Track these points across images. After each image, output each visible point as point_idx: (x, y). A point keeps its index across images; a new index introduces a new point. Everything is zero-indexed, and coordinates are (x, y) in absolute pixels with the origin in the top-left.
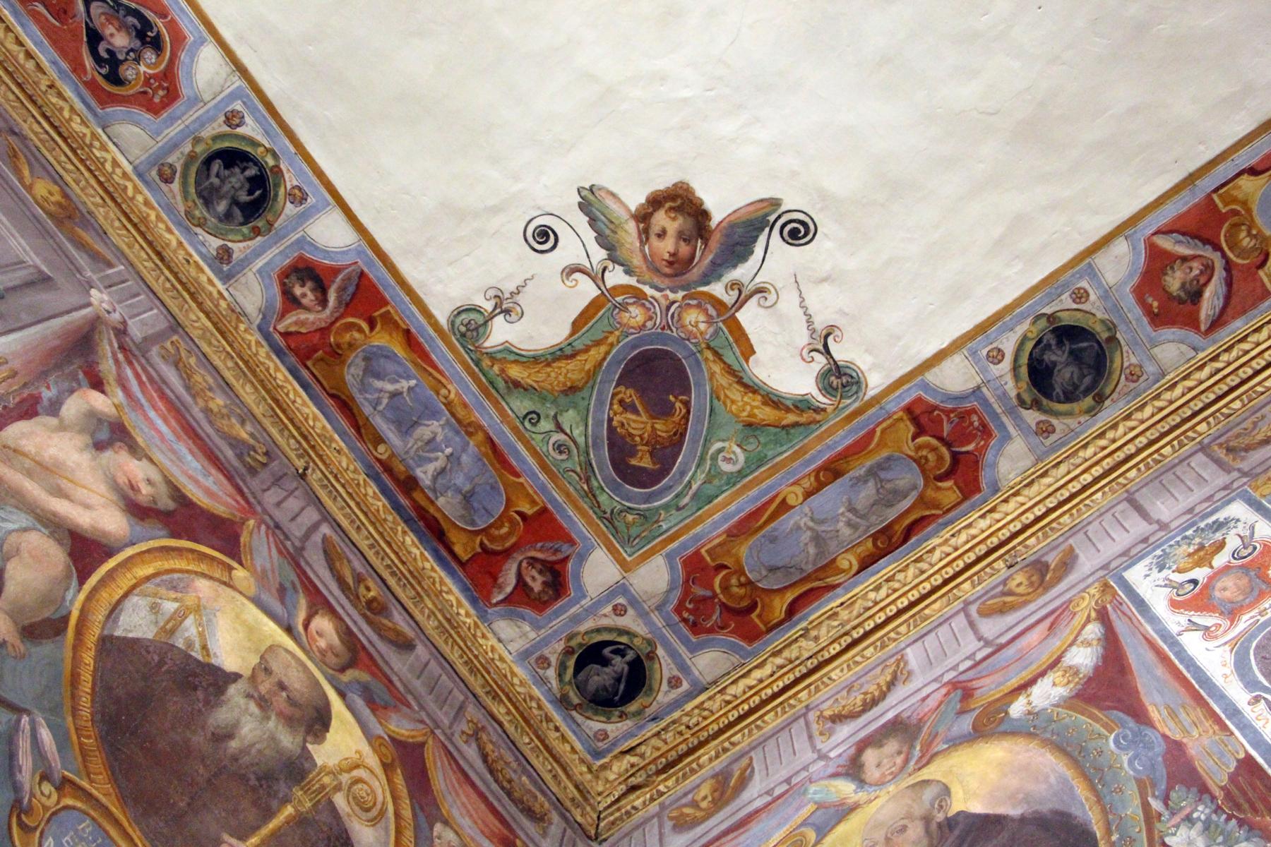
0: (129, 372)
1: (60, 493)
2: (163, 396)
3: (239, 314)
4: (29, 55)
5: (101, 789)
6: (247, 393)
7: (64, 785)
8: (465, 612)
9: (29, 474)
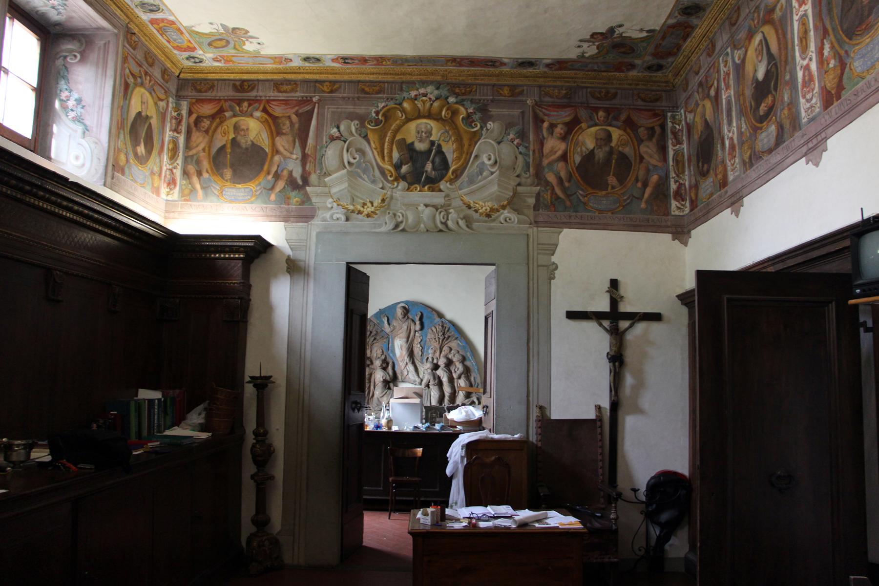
0: (544, 110)
1: (556, 152)
2: (550, 106)
3: (545, 72)
4: (481, 70)
5: (591, 191)
6: (558, 83)
7: (586, 196)
8: (622, 75)
9: (551, 156)
